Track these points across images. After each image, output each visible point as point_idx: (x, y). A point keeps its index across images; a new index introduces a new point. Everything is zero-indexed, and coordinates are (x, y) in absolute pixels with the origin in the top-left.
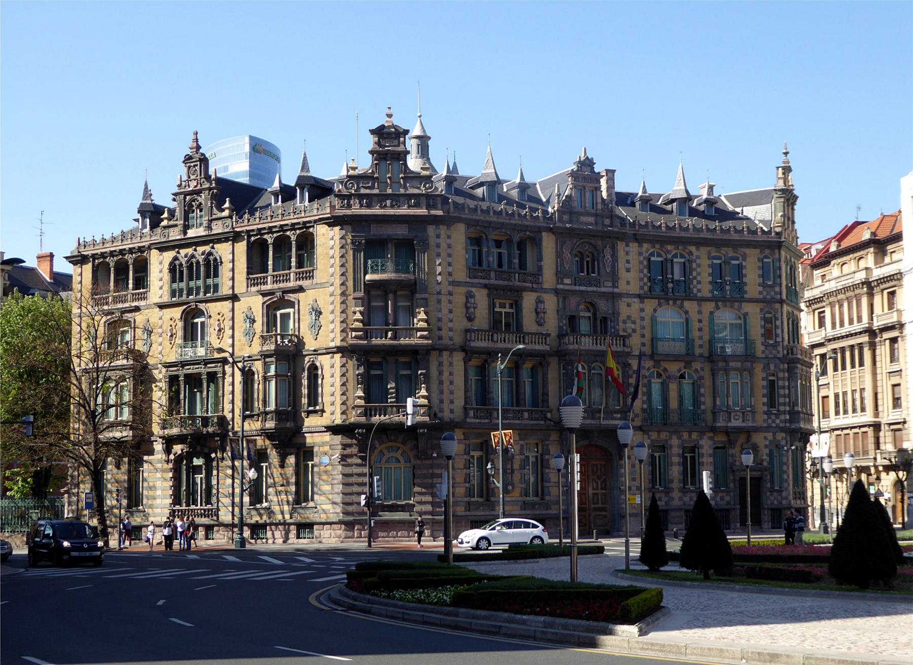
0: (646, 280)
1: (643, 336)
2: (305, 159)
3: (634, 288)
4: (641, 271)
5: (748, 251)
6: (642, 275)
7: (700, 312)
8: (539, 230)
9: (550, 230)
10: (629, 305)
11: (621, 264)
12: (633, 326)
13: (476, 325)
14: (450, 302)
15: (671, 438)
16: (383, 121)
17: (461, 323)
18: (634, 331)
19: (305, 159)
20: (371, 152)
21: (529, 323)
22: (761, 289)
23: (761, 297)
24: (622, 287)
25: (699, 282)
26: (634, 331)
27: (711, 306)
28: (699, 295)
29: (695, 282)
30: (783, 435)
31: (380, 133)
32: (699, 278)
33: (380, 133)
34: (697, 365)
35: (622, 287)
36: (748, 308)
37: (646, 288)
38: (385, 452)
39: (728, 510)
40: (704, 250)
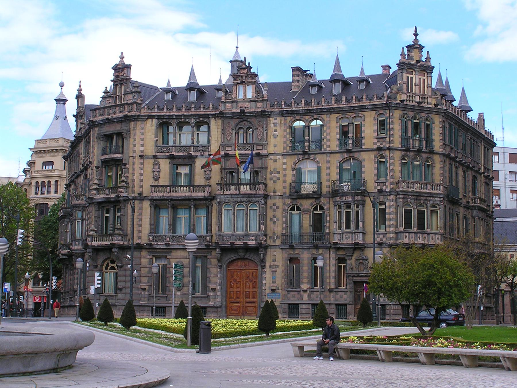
0: (288, 142)
1: (285, 182)
2: (463, 89)
3: (280, 149)
4: (285, 136)
5: (366, 113)
6: (285, 139)
7: (328, 162)
8: (207, 116)
9: (215, 116)
10: (275, 161)
11: (271, 132)
12: (277, 175)
13: (161, 182)
14: (142, 169)
15: (303, 253)
16: (117, 61)
17: (149, 181)
18: (278, 179)
19: (463, 89)
20: (112, 81)
21: (199, 179)
22: (376, 140)
23: (375, 147)
24: (271, 149)
25: (329, 140)
26: (278, 179)
27: (339, 157)
28: (328, 149)
29: (325, 140)
30: (388, 249)
31: (116, 68)
32: (328, 137)
33: (116, 68)
34: (323, 200)
35: (271, 149)
36: (364, 156)
37: (288, 148)
38: (110, 263)
39: (345, 305)
40: (334, 117)
